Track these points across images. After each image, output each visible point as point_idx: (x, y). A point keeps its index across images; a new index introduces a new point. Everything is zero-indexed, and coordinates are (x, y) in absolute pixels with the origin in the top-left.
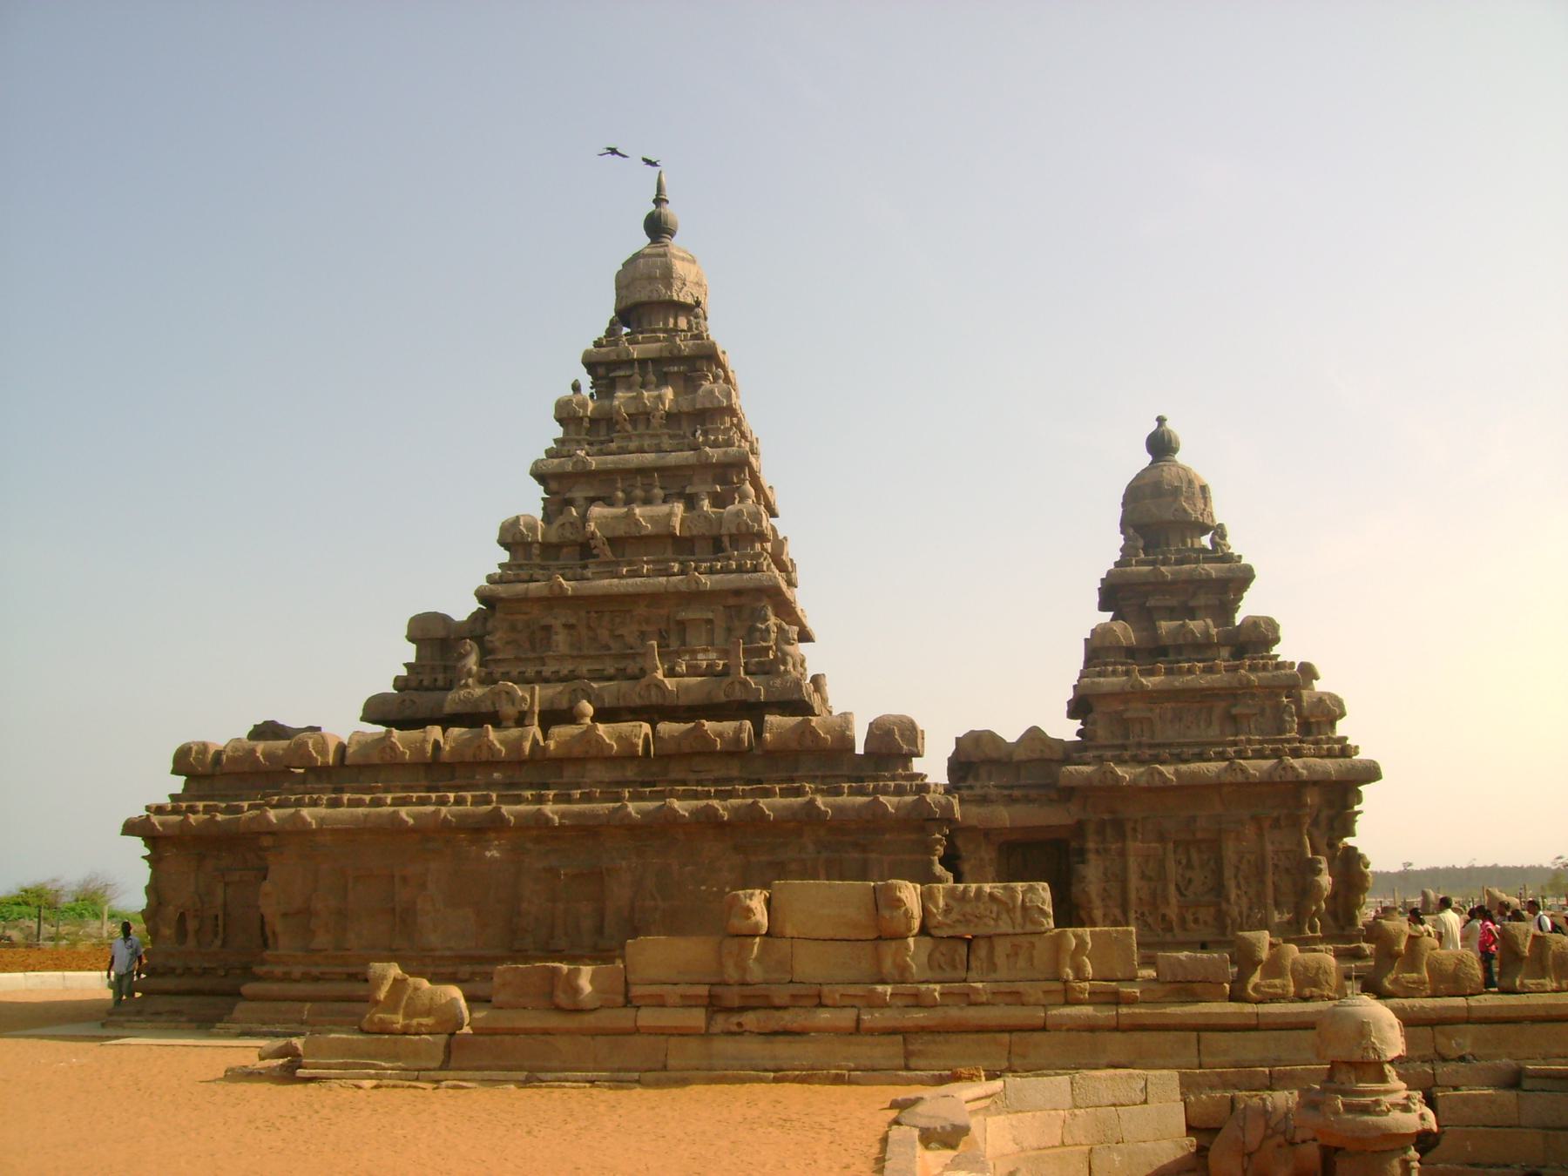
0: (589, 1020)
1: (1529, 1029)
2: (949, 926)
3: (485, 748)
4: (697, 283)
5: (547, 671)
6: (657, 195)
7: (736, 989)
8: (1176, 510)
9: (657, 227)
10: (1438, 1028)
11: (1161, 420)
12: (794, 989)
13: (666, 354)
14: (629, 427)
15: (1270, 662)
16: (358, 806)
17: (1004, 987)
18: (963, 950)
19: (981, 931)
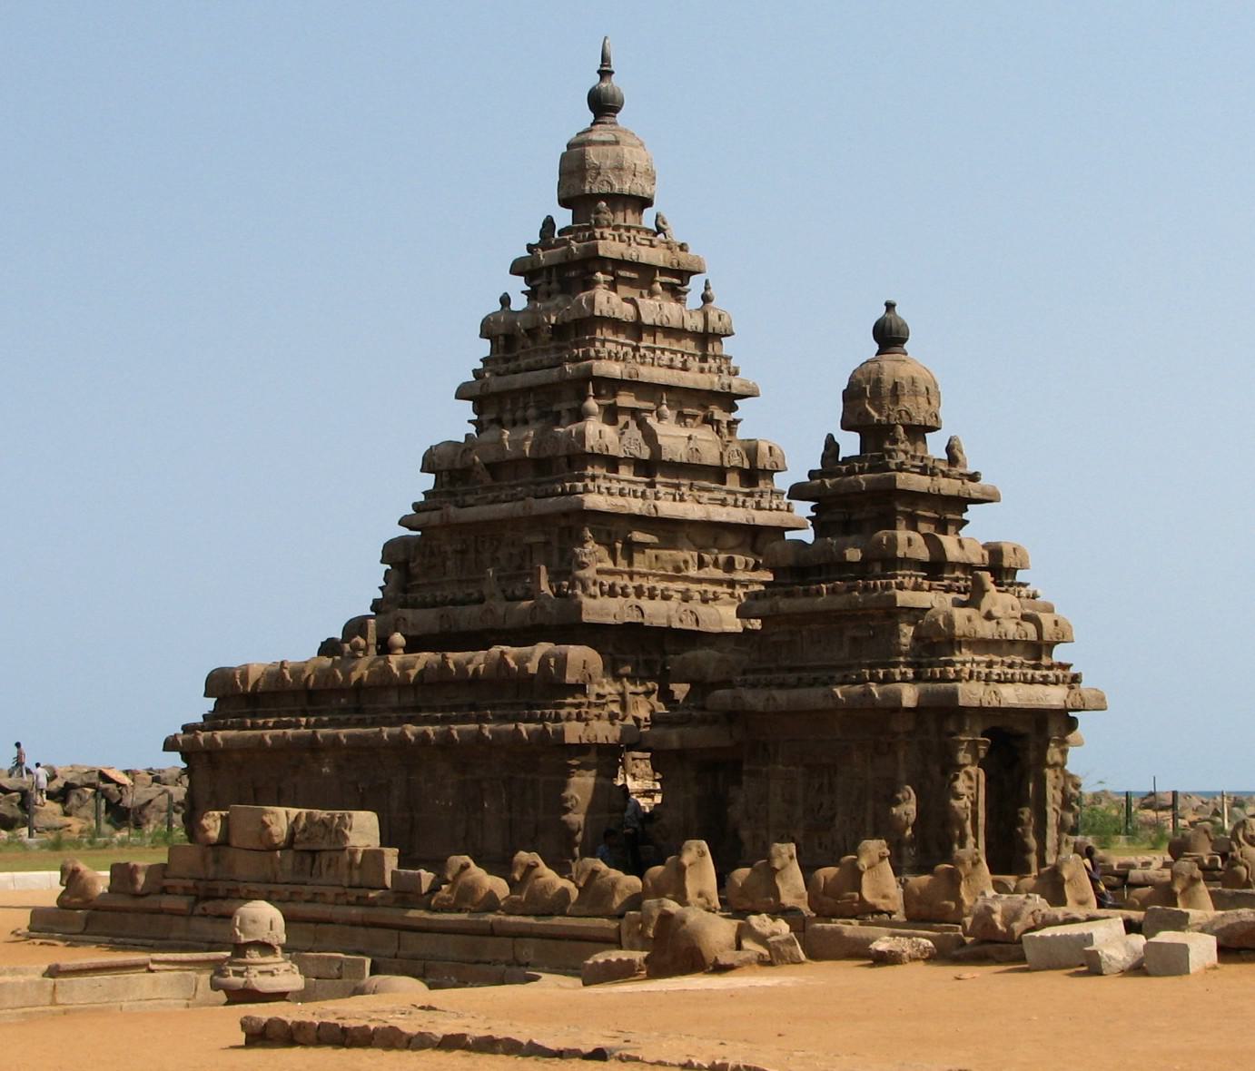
0: (142, 902)
1: (565, 945)
2: (301, 842)
3: (331, 678)
4: (616, 168)
5: (438, 593)
6: (602, 66)
7: (204, 883)
8: (860, 414)
9: (603, 105)
10: (519, 940)
11: (890, 306)
12: (230, 885)
13: (564, 260)
14: (529, 343)
15: (878, 582)
16: (289, 727)
17: (317, 890)
18: (309, 860)
19: (316, 847)
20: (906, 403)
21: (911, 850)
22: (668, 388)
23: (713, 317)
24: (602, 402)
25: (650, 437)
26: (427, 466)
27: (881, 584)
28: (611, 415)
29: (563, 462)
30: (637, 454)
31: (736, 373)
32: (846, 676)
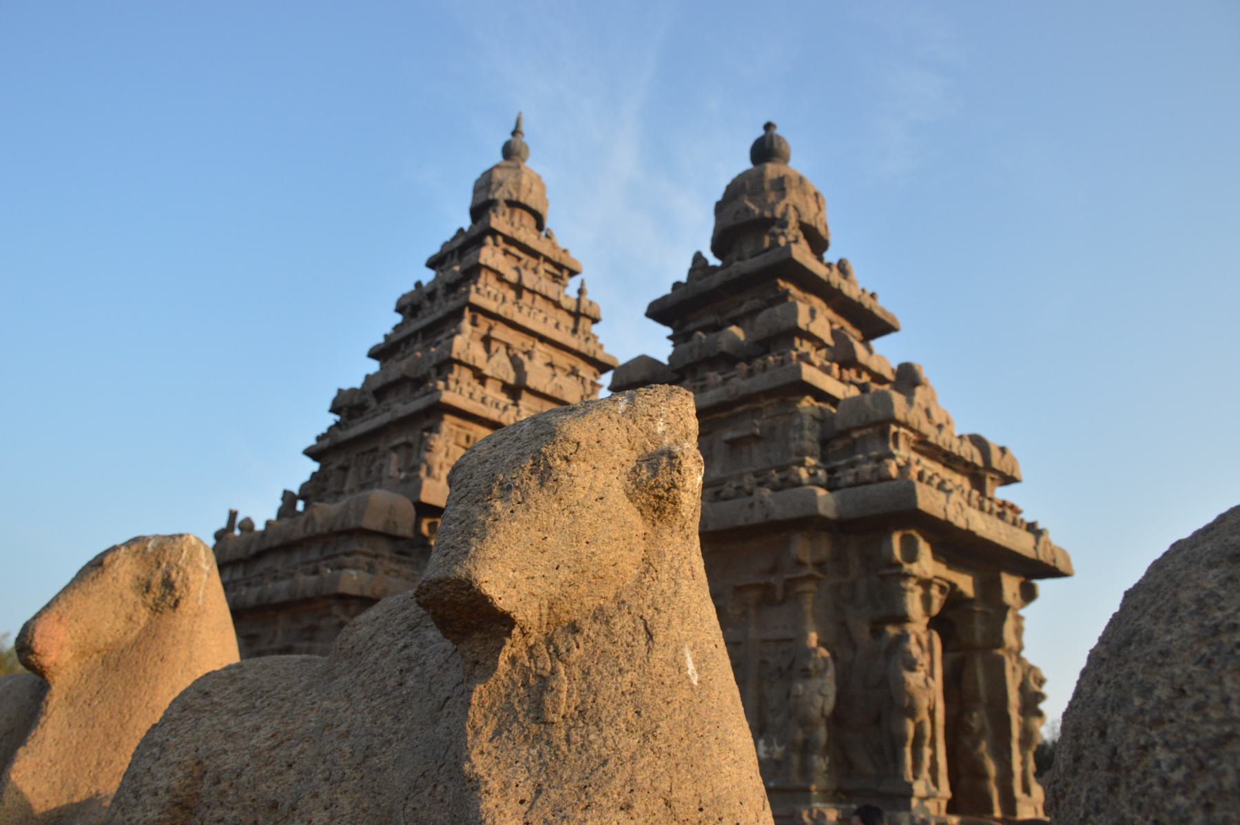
8: (738, 213)
11: (768, 126)
14: (427, 304)
20: (793, 197)
21: (822, 760)
22: (543, 339)
23: (584, 303)
24: (476, 329)
25: (518, 366)
26: (335, 409)
27: (775, 361)
28: (487, 341)
29: (433, 372)
30: (504, 378)
31: (601, 347)
32: (717, 493)
